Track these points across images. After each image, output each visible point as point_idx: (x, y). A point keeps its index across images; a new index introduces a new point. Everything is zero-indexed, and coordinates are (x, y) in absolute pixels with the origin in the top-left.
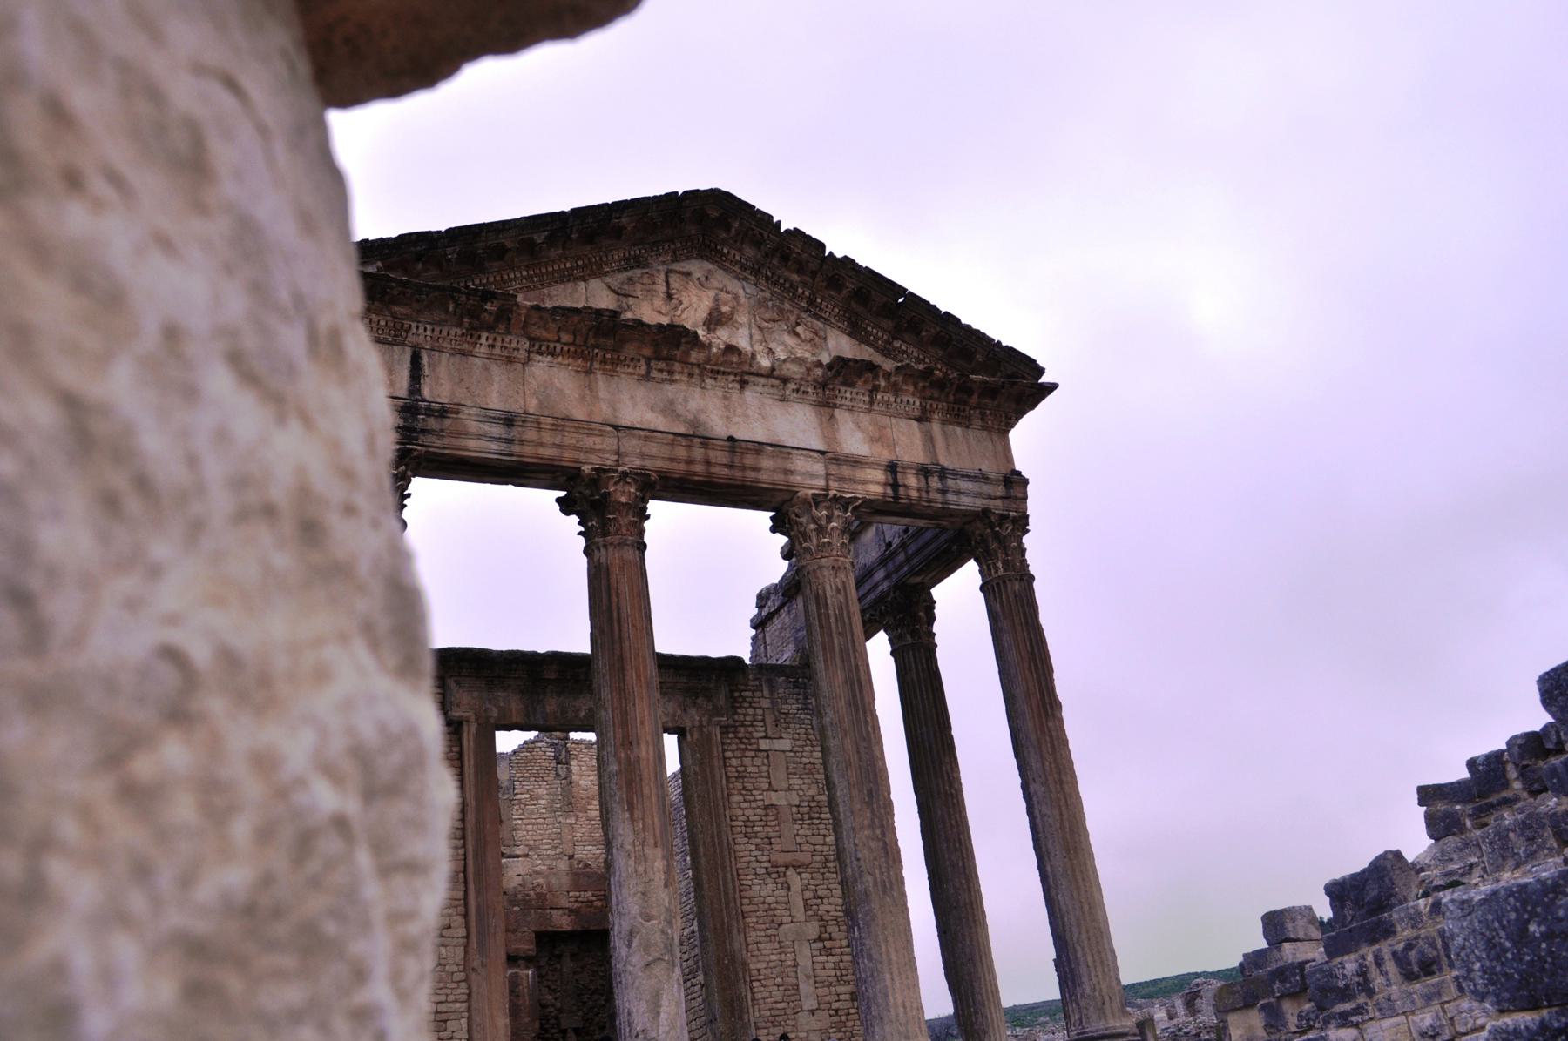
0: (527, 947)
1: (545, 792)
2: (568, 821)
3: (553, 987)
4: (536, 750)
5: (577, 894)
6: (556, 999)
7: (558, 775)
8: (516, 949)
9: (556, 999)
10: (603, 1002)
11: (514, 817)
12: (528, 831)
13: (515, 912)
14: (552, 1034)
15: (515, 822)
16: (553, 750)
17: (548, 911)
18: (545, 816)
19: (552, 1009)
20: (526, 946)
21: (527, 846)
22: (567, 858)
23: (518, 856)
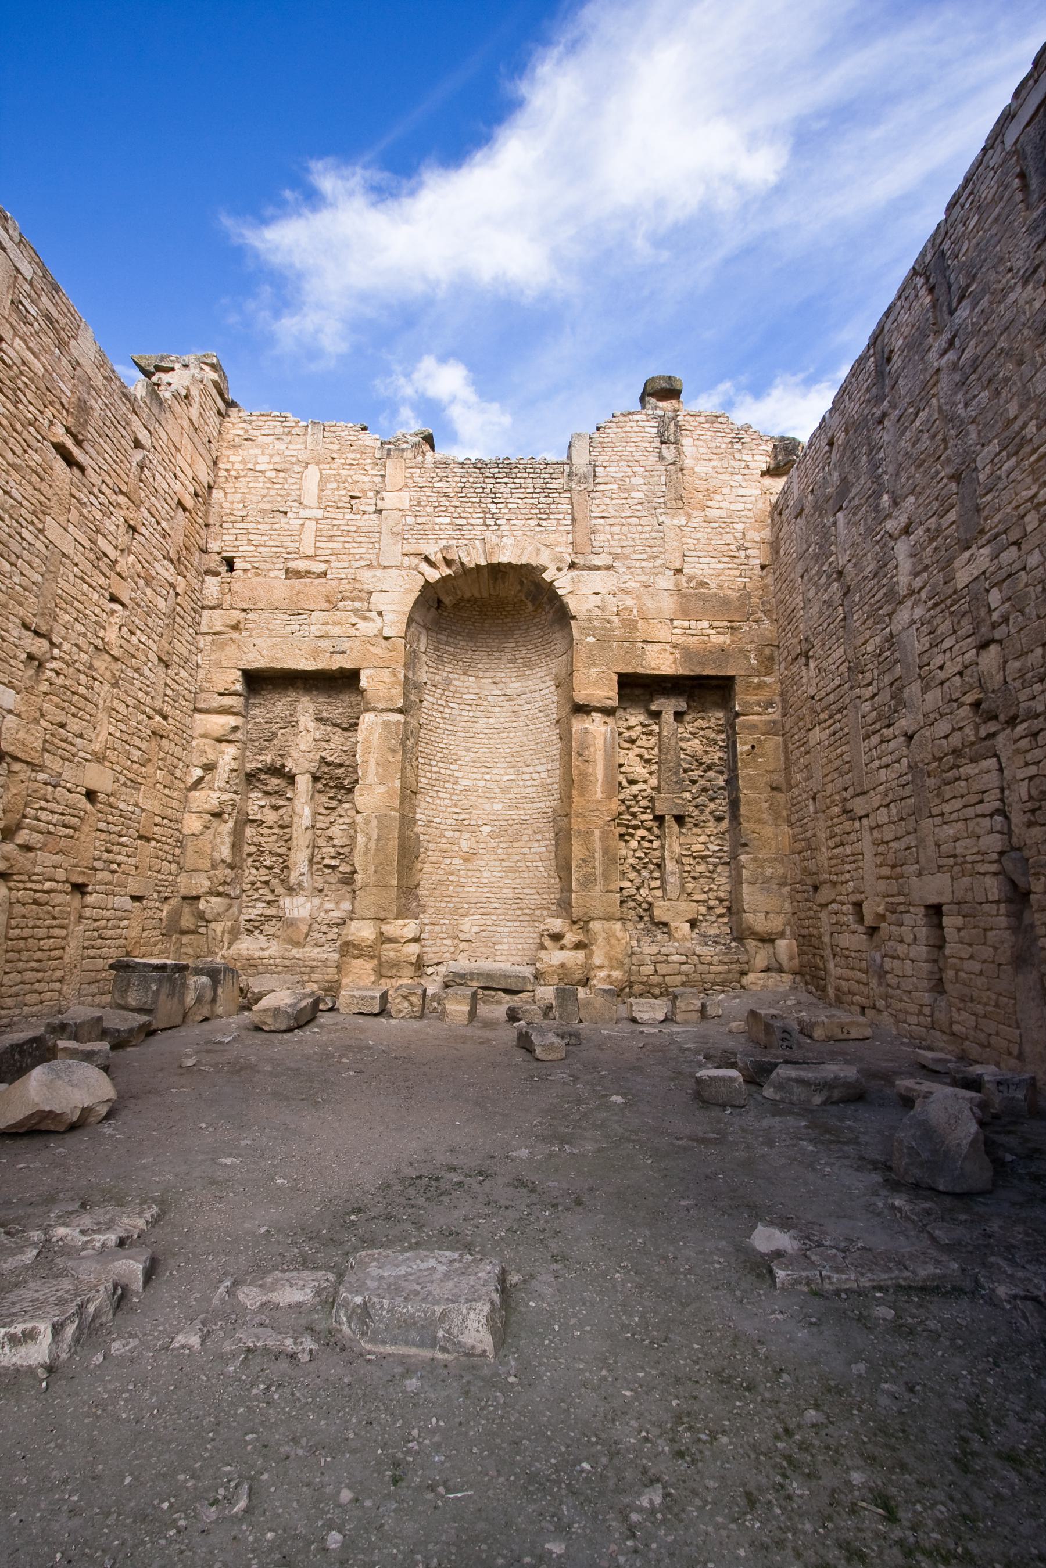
0: (606, 694)
1: (642, 481)
2: (676, 522)
3: (647, 757)
4: (629, 424)
5: (686, 624)
6: (651, 773)
7: (661, 458)
8: (588, 695)
9: (651, 773)
10: (723, 784)
11: (593, 515)
12: (613, 535)
13: (589, 644)
14: (642, 822)
15: (594, 522)
16: (656, 424)
17: (640, 645)
18: (639, 514)
19: (644, 787)
20: (607, 693)
21: (611, 554)
22: (671, 573)
23: (598, 568)
